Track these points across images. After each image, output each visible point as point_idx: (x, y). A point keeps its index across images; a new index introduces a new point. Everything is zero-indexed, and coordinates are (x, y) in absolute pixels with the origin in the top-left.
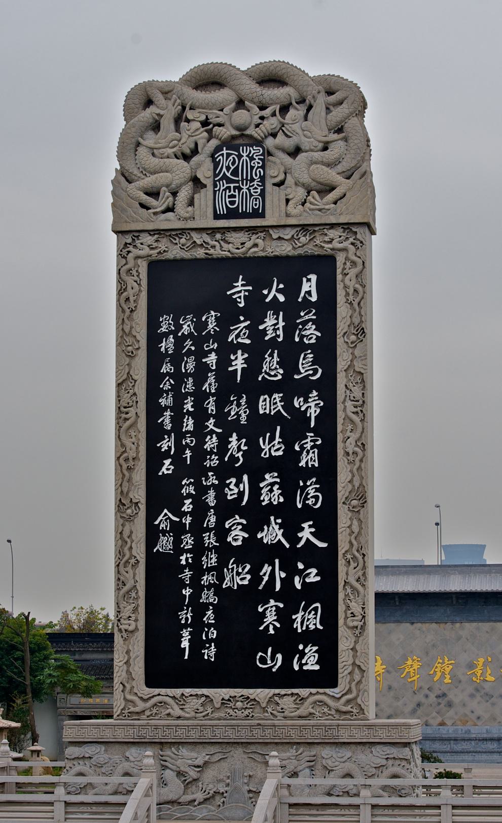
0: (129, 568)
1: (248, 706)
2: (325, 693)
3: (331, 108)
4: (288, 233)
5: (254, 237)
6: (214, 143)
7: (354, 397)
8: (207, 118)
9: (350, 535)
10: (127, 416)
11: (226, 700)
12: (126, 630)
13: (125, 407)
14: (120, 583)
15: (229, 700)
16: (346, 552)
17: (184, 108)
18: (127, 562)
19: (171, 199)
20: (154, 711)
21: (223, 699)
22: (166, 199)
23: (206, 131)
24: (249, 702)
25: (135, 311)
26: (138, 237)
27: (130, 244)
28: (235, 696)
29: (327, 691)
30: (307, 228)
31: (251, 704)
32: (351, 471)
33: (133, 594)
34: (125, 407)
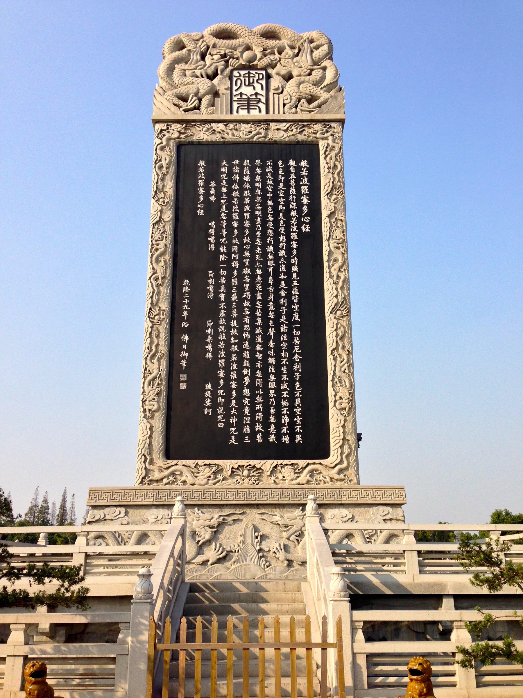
0: (155, 361)
1: (254, 474)
2: (320, 464)
3: (314, 50)
4: (283, 126)
5: (258, 128)
6: (230, 68)
7: (337, 237)
8: (225, 53)
9: (336, 336)
10: (158, 247)
11: (236, 469)
12: (150, 410)
13: (156, 241)
14: (147, 372)
15: (238, 469)
16: (334, 350)
17: (208, 48)
18: (153, 356)
19: (197, 101)
20: (171, 478)
21: (233, 468)
22: (192, 103)
23: (225, 61)
24: (255, 471)
25: (167, 175)
26: (171, 126)
27: (165, 130)
28: (243, 466)
29: (321, 461)
30: (296, 123)
31: (257, 472)
32: (336, 289)
33: (157, 381)
34: (156, 241)
